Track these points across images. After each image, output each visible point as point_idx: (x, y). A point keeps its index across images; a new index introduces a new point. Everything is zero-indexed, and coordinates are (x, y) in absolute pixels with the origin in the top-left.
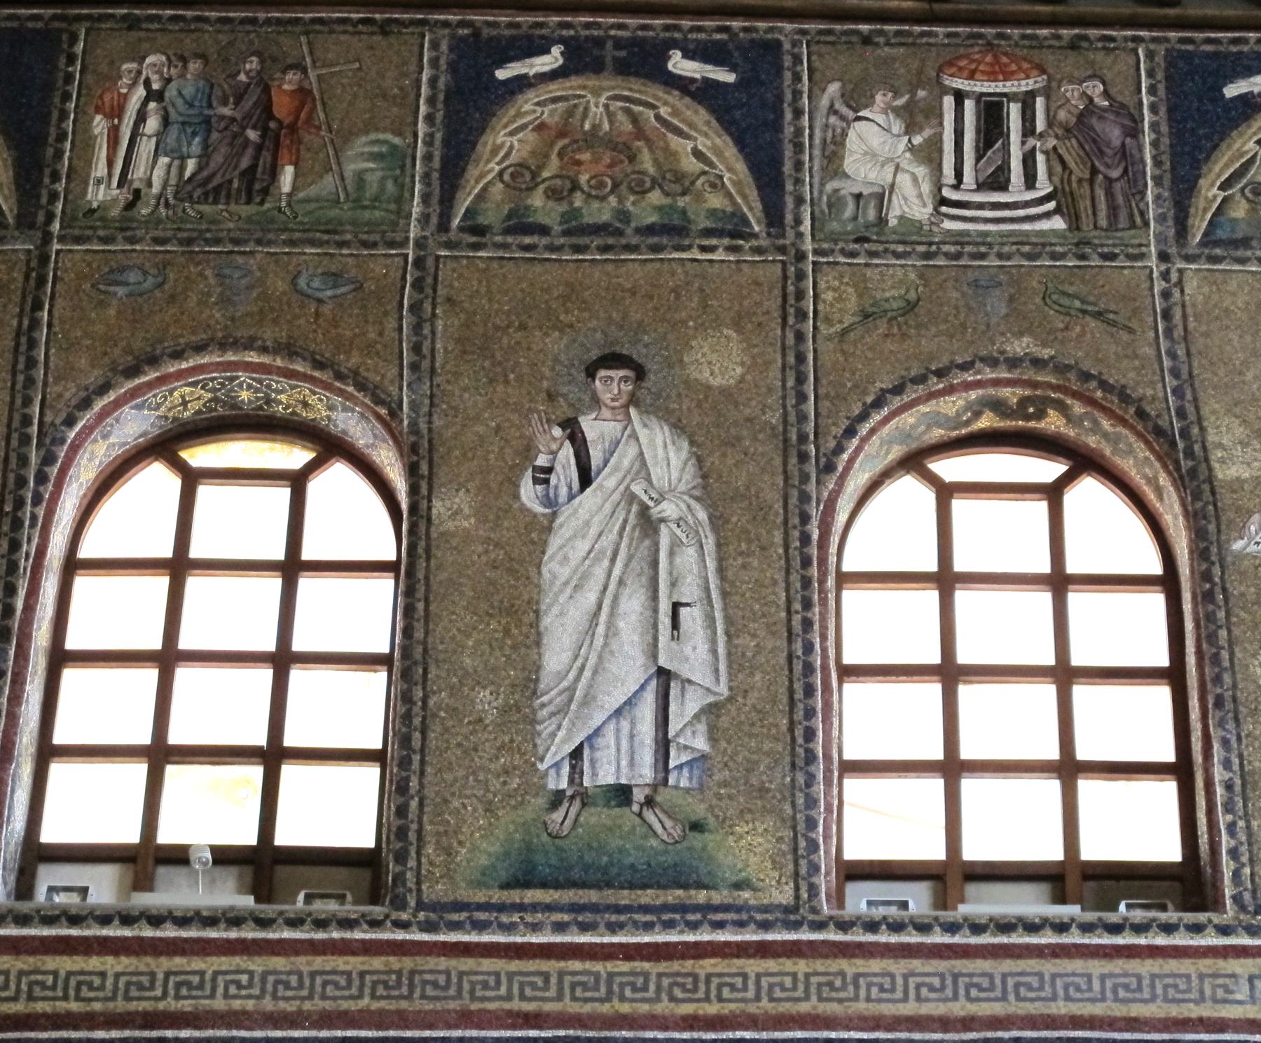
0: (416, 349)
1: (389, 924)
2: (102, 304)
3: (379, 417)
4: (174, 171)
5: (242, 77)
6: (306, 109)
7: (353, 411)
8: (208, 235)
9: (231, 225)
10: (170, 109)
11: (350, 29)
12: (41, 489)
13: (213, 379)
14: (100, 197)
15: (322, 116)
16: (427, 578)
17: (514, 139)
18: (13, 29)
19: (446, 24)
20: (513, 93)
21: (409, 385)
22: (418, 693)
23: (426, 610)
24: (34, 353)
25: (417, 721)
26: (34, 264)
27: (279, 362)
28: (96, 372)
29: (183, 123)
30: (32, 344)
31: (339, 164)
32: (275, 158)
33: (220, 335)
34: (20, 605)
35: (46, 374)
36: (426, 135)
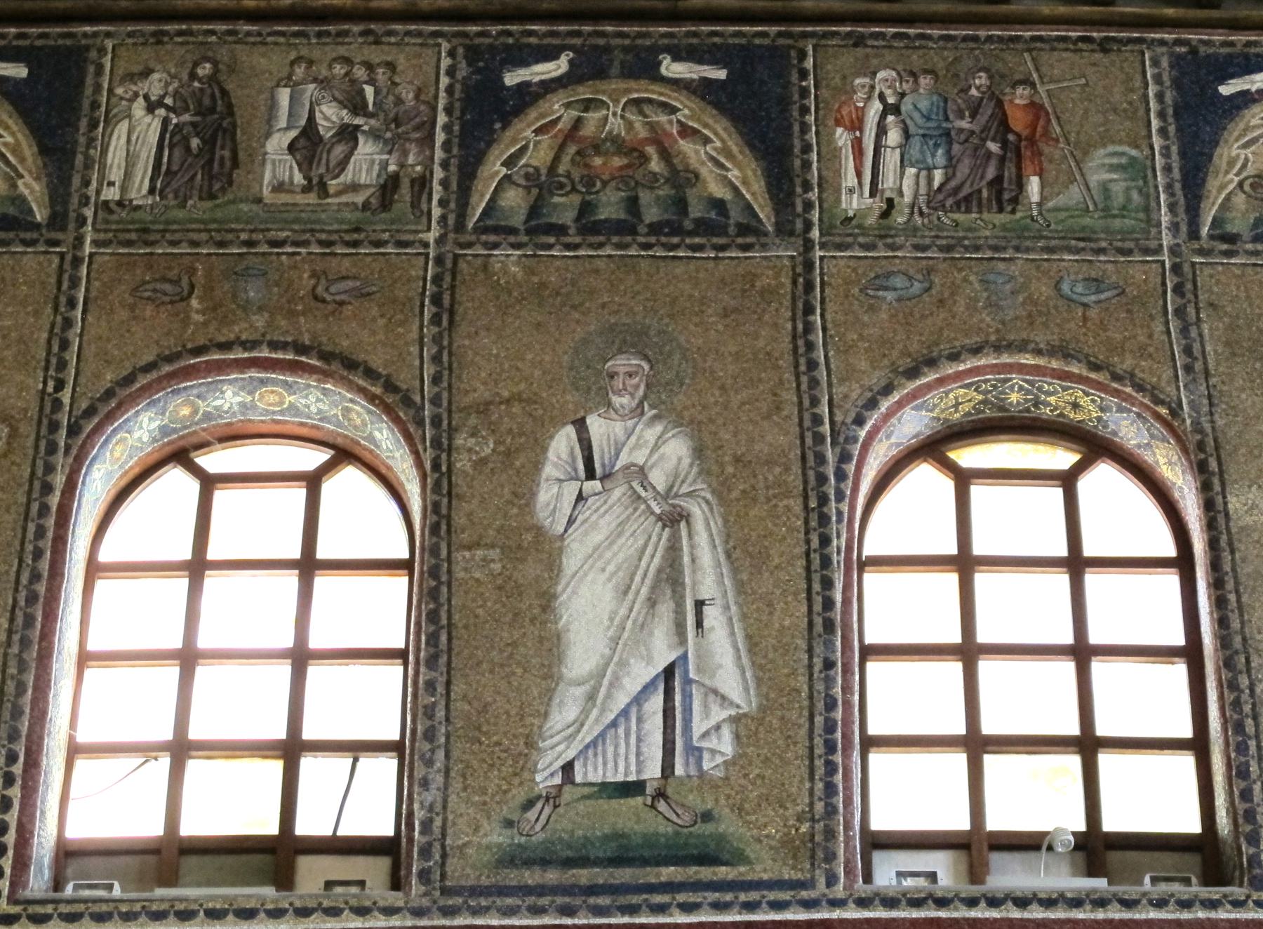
0: (1188, 351)
1: (1251, 903)
2: (872, 309)
3: (1158, 417)
4: (923, 182)
5: (974, 92)
6: (1042, 122)
7: (1130, 411)
8: (966, 242)
9: (988, 233)
10: (908, 122)
11: (1071, 46)
12: (842, 486)
13: (986, 381)
14: (855, 205)
15: (1058, 130)
16: (1234, 570)
17: (1248, 151)
18: (742, 46)
19: (1162, 42)
20: (1239, 108)
21: (1185, 386)
22: (1244, 681)
23: (1239, 601)
24: (814, 355)
25: (1247, 708)
26: (799, 269)
27: (1055, 364)
28: (877, 374)
29: (924, 136)
30: (810, 346)
31: (1083, 175)
32: (1019, 168)
33: (993, 338)
34: (838, 597)
35: (829, 375)
36: (1162, 148)
